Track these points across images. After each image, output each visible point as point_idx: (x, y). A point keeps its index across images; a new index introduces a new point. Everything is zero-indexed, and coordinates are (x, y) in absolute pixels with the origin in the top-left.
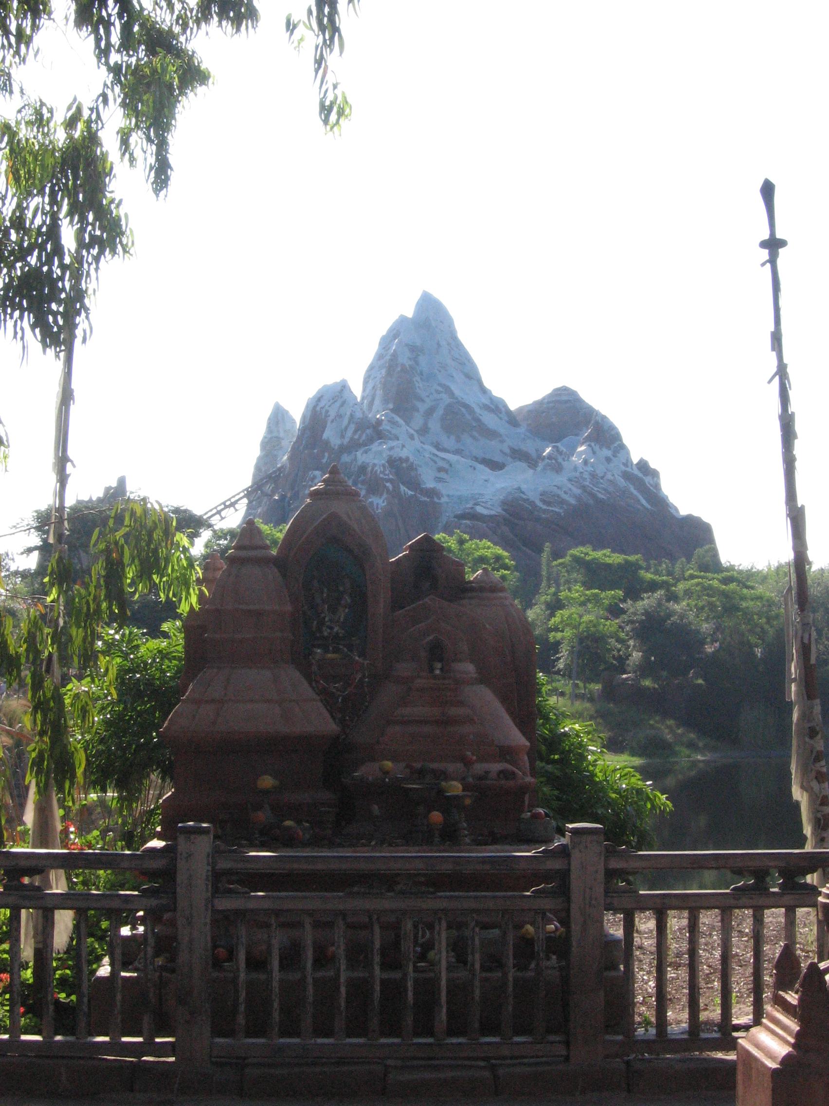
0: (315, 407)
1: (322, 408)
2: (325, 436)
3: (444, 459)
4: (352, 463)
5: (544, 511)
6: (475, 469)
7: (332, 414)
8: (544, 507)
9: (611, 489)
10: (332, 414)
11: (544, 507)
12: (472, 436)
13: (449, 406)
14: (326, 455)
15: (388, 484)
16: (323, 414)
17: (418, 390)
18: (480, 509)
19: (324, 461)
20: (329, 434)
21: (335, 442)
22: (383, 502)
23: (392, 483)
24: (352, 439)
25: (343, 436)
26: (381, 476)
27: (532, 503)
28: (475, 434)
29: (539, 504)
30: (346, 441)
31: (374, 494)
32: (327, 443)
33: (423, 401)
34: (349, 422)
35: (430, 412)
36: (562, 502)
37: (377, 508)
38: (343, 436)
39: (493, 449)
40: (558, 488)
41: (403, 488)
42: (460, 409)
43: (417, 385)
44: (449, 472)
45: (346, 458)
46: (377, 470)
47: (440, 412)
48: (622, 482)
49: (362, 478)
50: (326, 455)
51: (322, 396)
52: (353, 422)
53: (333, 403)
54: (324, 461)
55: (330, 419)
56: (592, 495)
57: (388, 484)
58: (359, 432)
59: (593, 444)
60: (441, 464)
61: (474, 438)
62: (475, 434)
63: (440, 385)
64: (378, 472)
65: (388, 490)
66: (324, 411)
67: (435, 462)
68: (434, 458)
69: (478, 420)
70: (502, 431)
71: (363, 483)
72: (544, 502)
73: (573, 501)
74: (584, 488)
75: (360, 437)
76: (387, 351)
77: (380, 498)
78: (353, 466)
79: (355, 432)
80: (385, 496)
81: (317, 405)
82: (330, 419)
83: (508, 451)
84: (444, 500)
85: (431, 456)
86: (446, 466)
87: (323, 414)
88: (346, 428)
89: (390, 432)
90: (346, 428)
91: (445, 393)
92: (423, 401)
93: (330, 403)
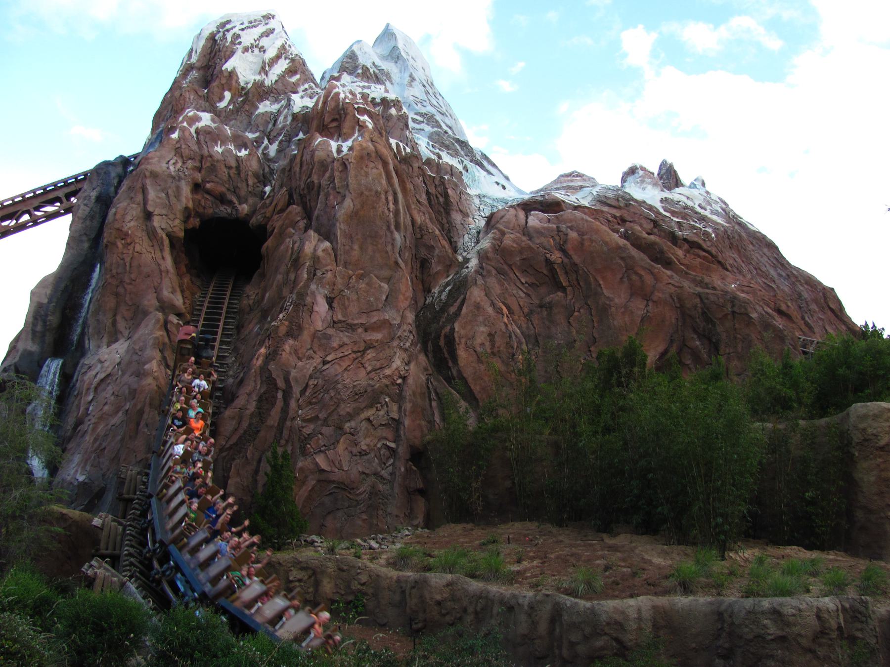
4: (279, 112)
6: (504, 188)
7: (248, 38)
10: (248, 38)
14: (228, 95)
15: (365, 118)
16: (229, 40)
19: (222, 105)
24: (282, 77)
25: (264, 69)
32: (232, 74)
34: (278, 57)
38: (264, 69)
40: (688, 198)
42: (453, 144)
45: (266, 107)
46: (338, 94)
50: (228, 95)
51: (229, 22)
53: (248, 27)
54: (222, 105)
63: (421, 115)
65: (362, 126)
66: (229, 36)
72: (673, 213)
78: (281, 118)
85: (431, 148)
87: (229, 40)
91: (428, 125)
93: (243, 27)
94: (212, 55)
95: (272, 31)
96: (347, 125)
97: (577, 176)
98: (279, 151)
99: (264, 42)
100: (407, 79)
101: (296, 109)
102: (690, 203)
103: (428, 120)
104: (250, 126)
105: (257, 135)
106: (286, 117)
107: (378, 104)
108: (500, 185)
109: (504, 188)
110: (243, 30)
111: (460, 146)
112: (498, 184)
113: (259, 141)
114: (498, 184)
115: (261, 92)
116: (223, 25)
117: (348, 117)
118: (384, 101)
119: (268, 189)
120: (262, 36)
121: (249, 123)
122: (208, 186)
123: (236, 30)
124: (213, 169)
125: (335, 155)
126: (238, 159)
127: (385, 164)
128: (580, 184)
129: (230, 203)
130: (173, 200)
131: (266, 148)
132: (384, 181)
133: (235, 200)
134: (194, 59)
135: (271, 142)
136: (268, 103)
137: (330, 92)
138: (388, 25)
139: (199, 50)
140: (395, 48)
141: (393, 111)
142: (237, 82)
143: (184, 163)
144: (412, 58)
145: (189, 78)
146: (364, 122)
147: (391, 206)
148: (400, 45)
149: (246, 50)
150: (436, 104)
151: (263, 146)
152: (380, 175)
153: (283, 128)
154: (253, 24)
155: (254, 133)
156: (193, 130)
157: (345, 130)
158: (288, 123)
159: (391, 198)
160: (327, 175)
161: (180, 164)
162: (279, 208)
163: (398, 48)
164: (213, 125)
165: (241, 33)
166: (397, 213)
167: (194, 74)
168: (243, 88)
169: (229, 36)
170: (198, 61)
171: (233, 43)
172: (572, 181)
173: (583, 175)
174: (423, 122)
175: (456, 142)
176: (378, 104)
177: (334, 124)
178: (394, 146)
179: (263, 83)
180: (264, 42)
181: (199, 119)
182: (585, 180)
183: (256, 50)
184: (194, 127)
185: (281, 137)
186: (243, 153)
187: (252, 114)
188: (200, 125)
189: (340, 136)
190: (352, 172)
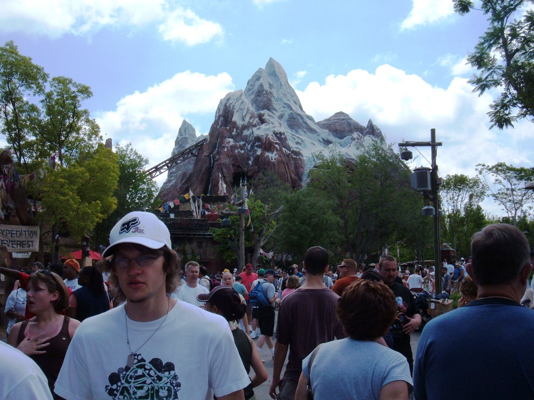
0: (226, 104)
1: (231, 104)
2: (233, 119)
3: (298, 138)
4: (250, 135)
6: (314, 145)
10: (237, 107)
12: (303, 131)
13: (291, 113)
14: (235, 130)
15: (277, 146)
16: (232, 107)
17: (274, 105)
19: (234, 133)
20: (236, 118)
21: (240, 123)
22: (275, 155)
23: (278, 145)
26: (272, 140)
28: (305, 130)
30: (246, 123)
31: (268, 152)
32: (235, 123)
33: (277, 111)
34: (247, 113)
37: (272, 159)
41: (284, 149)
42: (297, 117)
43: (273, 103)
44: (302, 145)
45: (246, 133)
46: (269, 138)
47: (286, 117)
49: (257, 144)
50: (235, 130)
52: (249, 113)
55: (237, 109)
57: (277, 146)
58: (253, 119)
59: (371, 136)
60: (298, 140)
61: (305, 132)
62: (305, 130)
64: (270, 138)
67: (295, 139)
68: (294, 137)
70: (318, 130)
71: (258, 146)
75: (253, 122)
76: (253, 86)
77: (272, 153)
78: (251, 137)
79: (251, 118)
80: (275, 152)
81: (227, 102)
82: (235, 111)
83: (321, 140)
84: (305, 158)
86: (301, 142)
87: (232, 107)
88: (246, 115)
89: (269, 120)
90: (246, 115)
91: (288, 108)
92: (277, 111)
93: (235, 102)
94: (227, 112)
95: (243, 102)
96: (272, 148)
97: (342, 114)
98: (251, 148)
99: (242, 107)
100: (280, 85)
101: (255, 135)
103: (288, 106)
104: (242, 140)
105: (244, 142)
106: (252, 137)
107: (278, 134)
108: (313, 145)
109: (314, 145)
110: (235, 103)
111: (299, 116)
112: (312, 143)
113: (244, 145)
114: (312, 143)
115: (244, 127)
116: (228, 100)
117: (273, 146)
118: (280, 133)
119: (250, 162)
120: (240, 105)
121: (242, 139)
122: (236, 164)
123: (233, 104)
124: (236, 159)
125: (271, 160)
126: (241, 154)
127: (284, 163)
128: (342, 118)
129: (241, 168)
130: (230, 172)
131: (247, 147)
132: (284, 169)
133: (242, 167)
134: (221, 113)
135: (248, 145)
136: (246, 131)
137: (267, 137)
138: (271, 57)
139: (222, 110)
140: (274, 71)
141: (283, 136)
142: (237, 125)
143: (229, 159)
144: (281, 74)
145: (220, 121)
146: (277, 147)
147: (286, 176)
148: (277, 70)
149: (237, 111)
150: (290, 92)
151: (246, 146)
152: (283, 168)
153: (252, 140)
154: (238, 100)
155: (243, 142)
156: (229, 146)
157: (272, 150)
158: (253, 139)
159: (286, 174)
160: (269, 167)
161: (228, 159)
162: (256, 172)
163: (275, 71)
164: (234, 144)
165: (235, 104)
166: (287, 177)
167: (222, 119)
168: (239, 127)
169: (231, 106)
170: (222, 113)
171: (233, 108)
172: (340, 116)
173: (344, 113)
174: (286, 107)
175: (297, 115)
176: (278, 134)
177: (269, 148)
178: (284, 152)
179: (244, 124)
181: (229, 142)
182: (344, 116)
183: (240, 110)
184: (229, 145)
185: (251, 144)
186: (243, 152)
187: (242, 135)
189: (270, 151)
190: (276, 167)
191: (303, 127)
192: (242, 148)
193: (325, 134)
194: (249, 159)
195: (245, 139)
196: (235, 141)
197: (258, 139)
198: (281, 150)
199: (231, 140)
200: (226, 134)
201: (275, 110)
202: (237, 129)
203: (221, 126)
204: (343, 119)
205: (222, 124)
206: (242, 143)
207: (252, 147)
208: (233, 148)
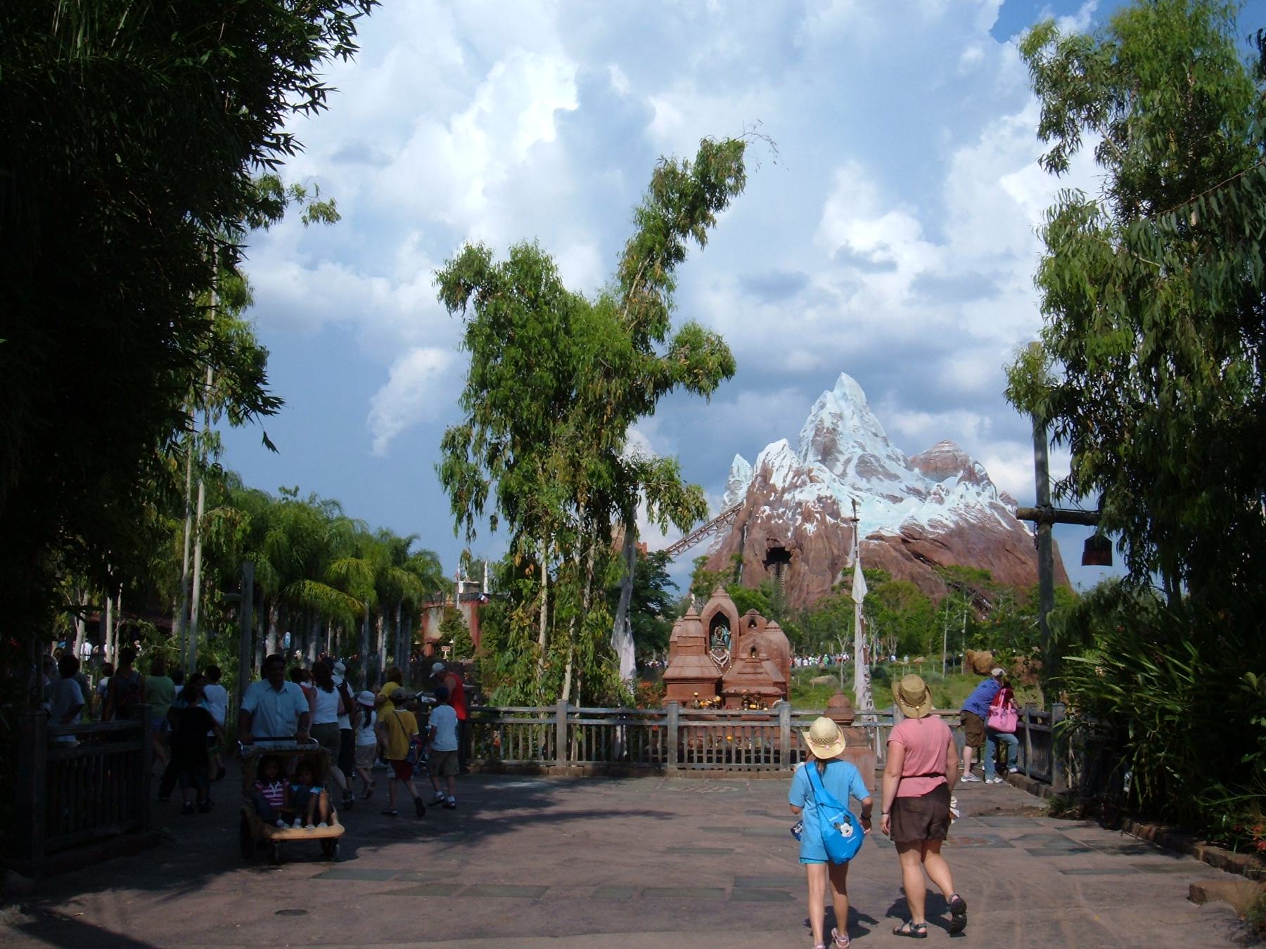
2: (771, 482)
5: (932, 533)
8: (931, 530)
9: (979, 516)
10: (777, 464)
11: (931, 530)
13: (862, 456)
15: (817, 515)
18: (884, 533)
20: (777, 480)
21: (779, 485)
24: (791, 483)
25: (784, 481)
27: (922, 527)
29: (928, 528)
32: (774, 486)
35: (848, 461)
36: (946, 526)
39: (895, 488)
41: (828, 518)
47: (855, 461)
48: (988, 511)
56: (966, 520)
57: (817, 515)
61: (881, 480)
63: (856, 442)
69: (882, 467)
71: (799, 514)
72: (931, 526)
73: (952, 525)
74: (960, 515)
79: (793, 478)
82: (775, 469)
83: (905, 489)
102: (941, 519)
104: (781, 506)
113: (784, 513)
115: (784, 491)
119: (789, 534)
167: (759, 479)
180: (784, 463)
181: (765, 511)
186: (781, 521)
188: (766, 514)
191: (880, 473)
192: (780, 517)
193: (914, 478)
194: (787, 530)
195: (786, 505)
196: (772, 508)
197: (799, 504)
198: (823, 520)
199: (767, 508)
200: (761, 499)
201: (841, 453)
202: (776, 493)
203: (758, 489)
204: (948, 452)
205: (760, 486)
206: (781, 510)
207: (794, 515)
208: (769, 517)
